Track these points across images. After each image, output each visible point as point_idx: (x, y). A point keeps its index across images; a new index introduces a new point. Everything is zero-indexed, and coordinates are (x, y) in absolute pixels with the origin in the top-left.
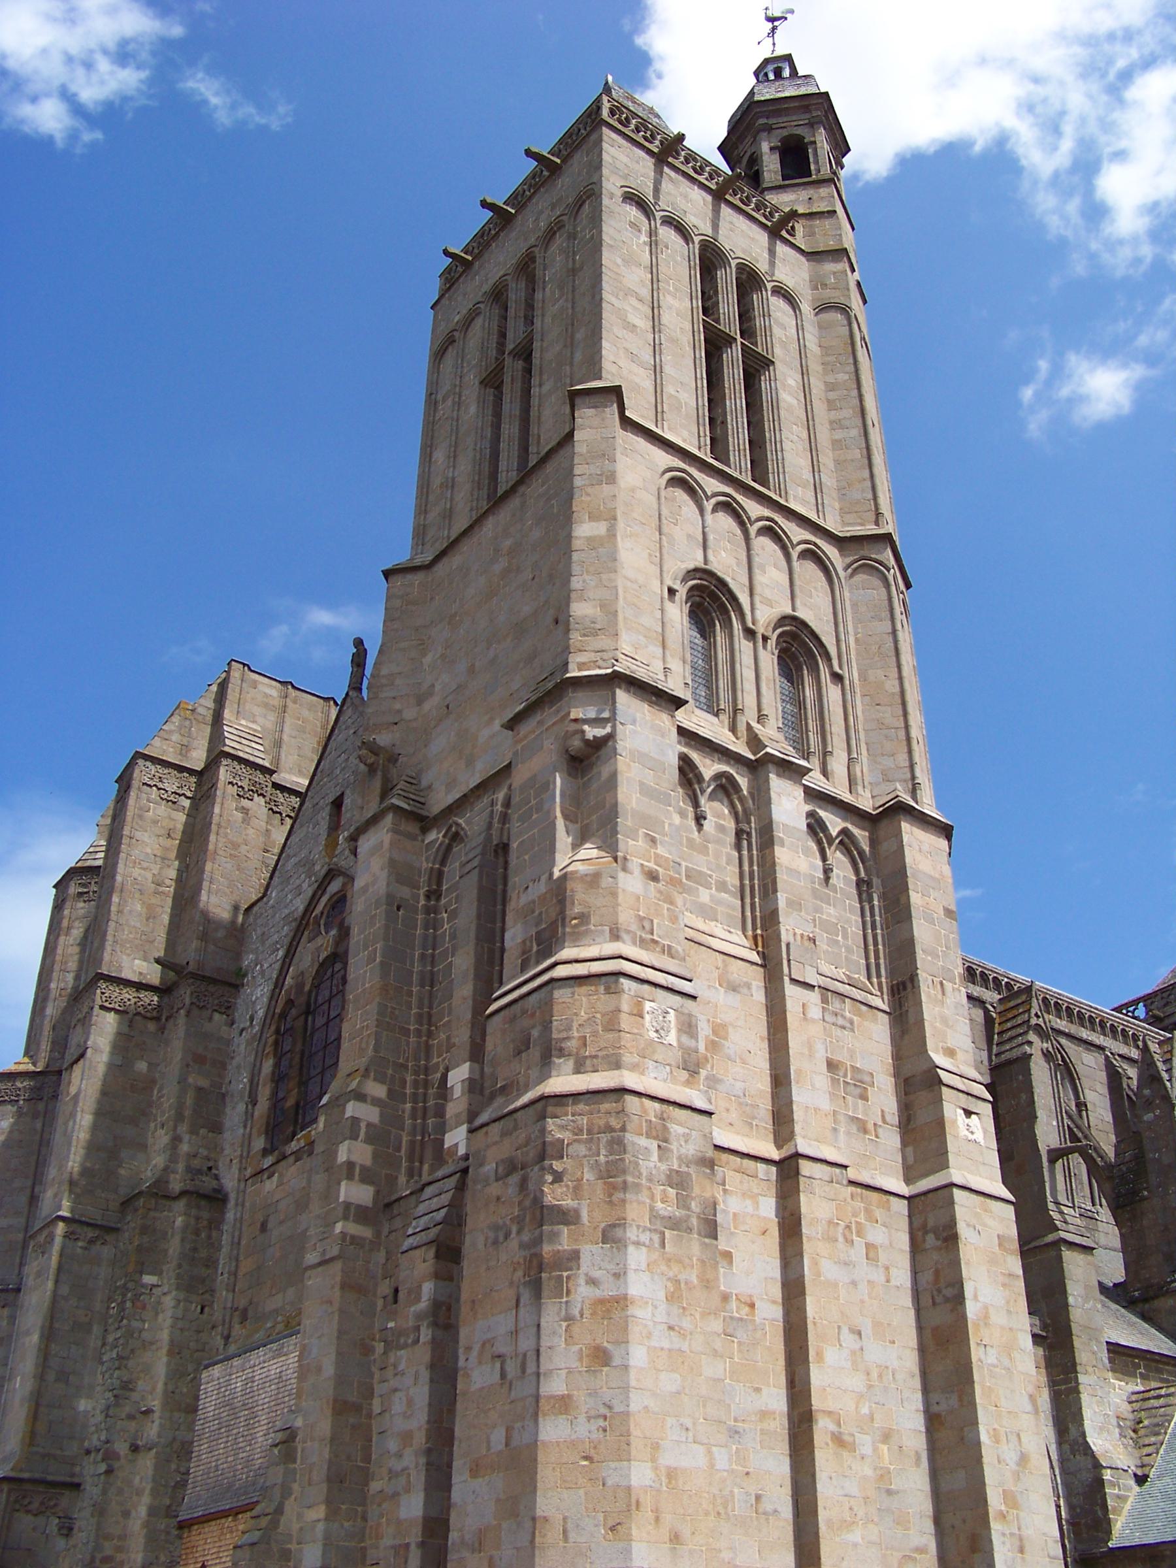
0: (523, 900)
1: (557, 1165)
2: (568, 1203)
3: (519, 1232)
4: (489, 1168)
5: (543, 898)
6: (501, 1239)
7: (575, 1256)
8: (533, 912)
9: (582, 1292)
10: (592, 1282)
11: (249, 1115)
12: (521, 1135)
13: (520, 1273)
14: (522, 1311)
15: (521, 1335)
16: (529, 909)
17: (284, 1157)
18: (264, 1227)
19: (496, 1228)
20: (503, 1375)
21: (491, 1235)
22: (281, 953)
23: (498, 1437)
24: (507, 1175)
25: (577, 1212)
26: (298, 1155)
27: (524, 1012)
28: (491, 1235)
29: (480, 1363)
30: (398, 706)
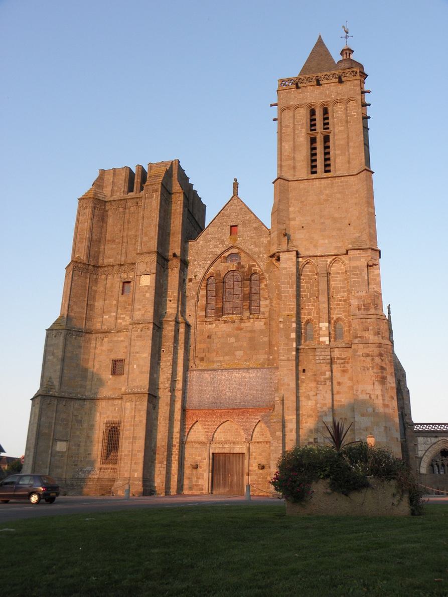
0: (357, 294)
1: (383, 358)
2: (384, 366)
3: (372, 369)
4: (360, 353)
5: (365, 297)
6: (366, 370)
7: (386, 377)
8: (361, 298)
9: (388, 384)
10: (390, 383)
11: (196, 305)
12: (371, 349)
13: (373, 378)
14: (375, 386)
15: (376, 391)
16: (359, 298)
17: (219, 320)
18: (209, 337)
19: (364, 367)
20: (370, 398)
21: (363, 368)
22: (209, 262)
23: (370, 410)
24: (367, 356)
25: (386, 368)
26: (225, 322)
27: (366, 322)
28: (363, 368)
29: (362, 394)
30: (284, 219)
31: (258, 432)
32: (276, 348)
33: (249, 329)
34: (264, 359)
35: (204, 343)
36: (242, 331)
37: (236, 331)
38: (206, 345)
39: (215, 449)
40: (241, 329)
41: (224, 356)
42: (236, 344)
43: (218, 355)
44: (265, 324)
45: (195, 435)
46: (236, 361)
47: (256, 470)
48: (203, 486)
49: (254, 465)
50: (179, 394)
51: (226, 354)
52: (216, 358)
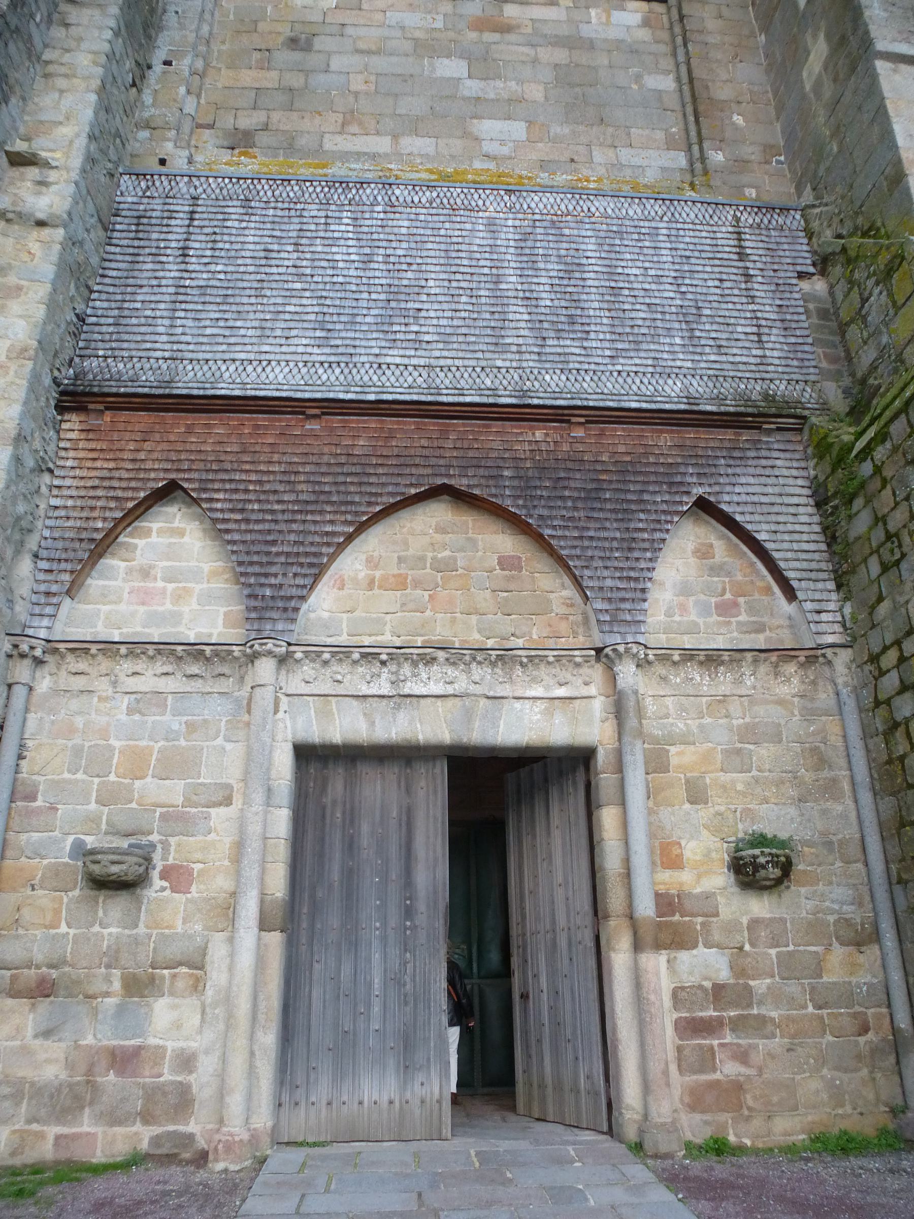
31: (685, 590)
32: (738, 119)
33: (547, 30)
34: (663, 169)
35: (265, 65)
36: (512, 37)
37: (473, 35)
38: (274, 74)
39: (325, 714)
40: (505, 28)
41: (395, 137)
42: (472, 87)
43: (354, 129)
44: (646, 23)
45: (145, 597)
46: (478, 165)
47: (708, 896)
48: (186, 1062)
49: (692, 849)
50: (35, 247)
51: (415, 126)
52: (339, 139)
